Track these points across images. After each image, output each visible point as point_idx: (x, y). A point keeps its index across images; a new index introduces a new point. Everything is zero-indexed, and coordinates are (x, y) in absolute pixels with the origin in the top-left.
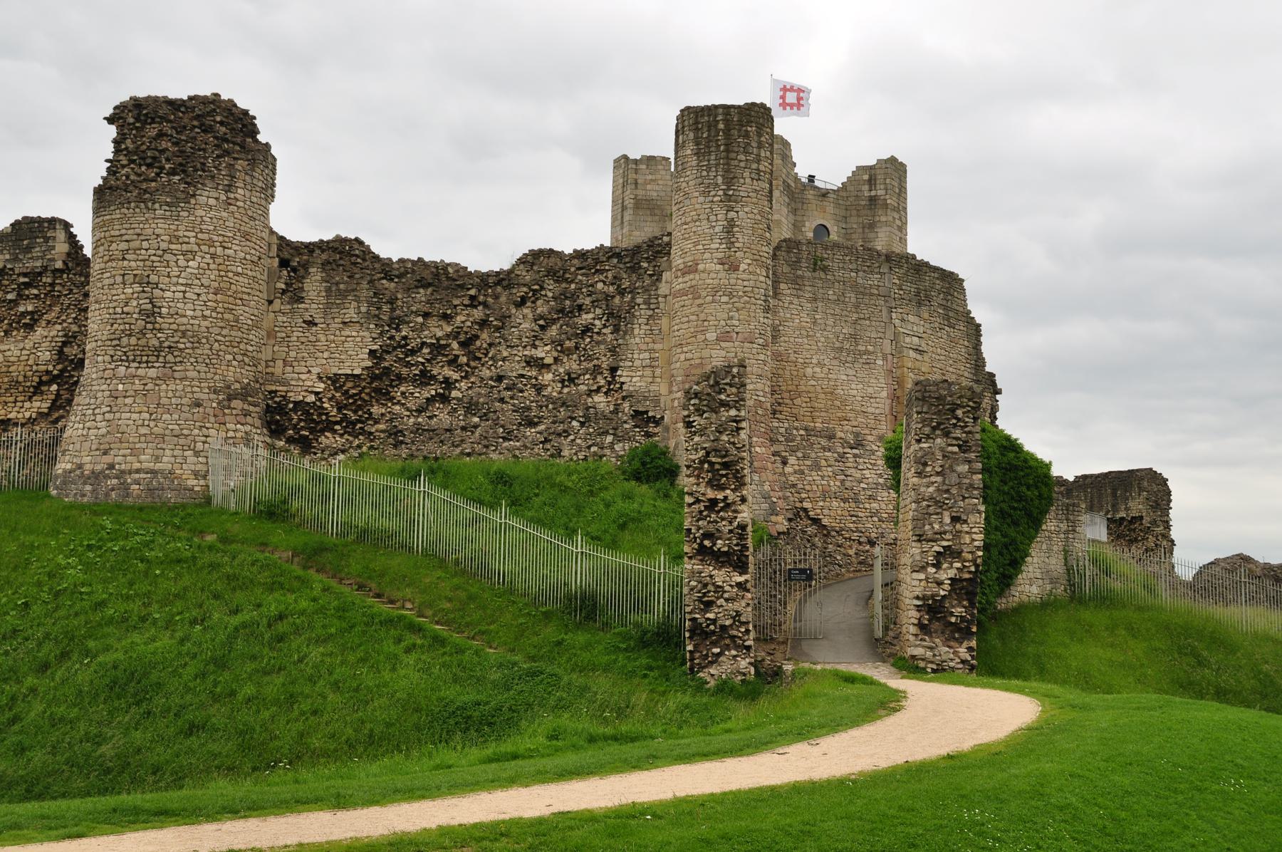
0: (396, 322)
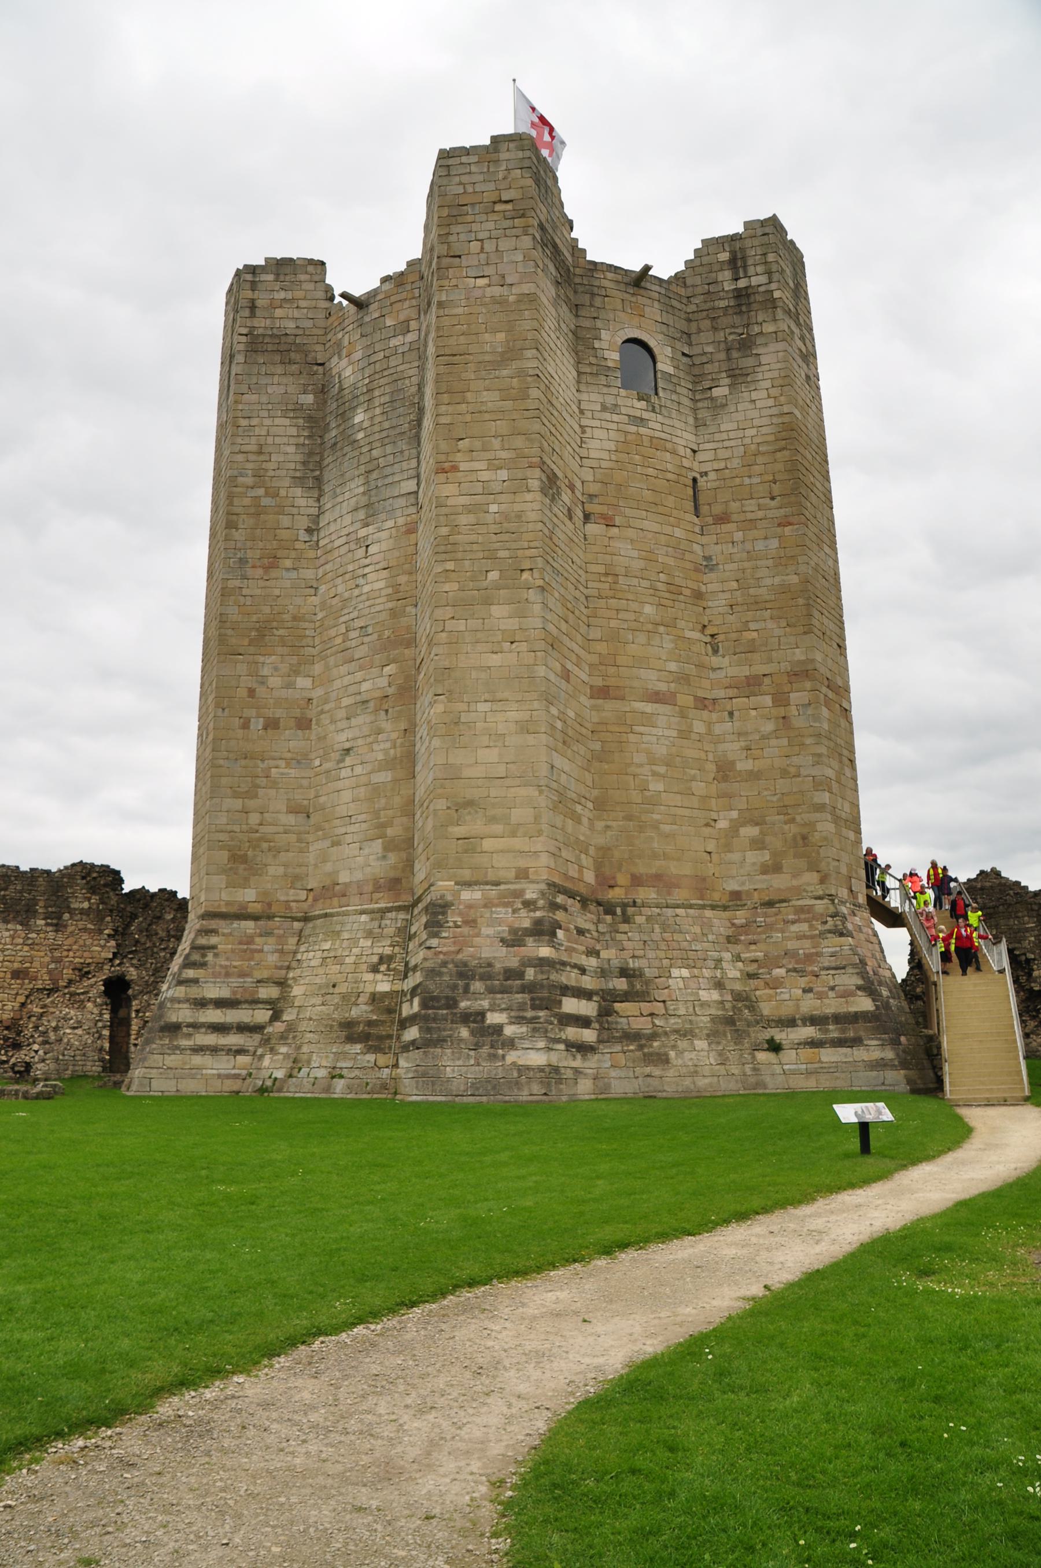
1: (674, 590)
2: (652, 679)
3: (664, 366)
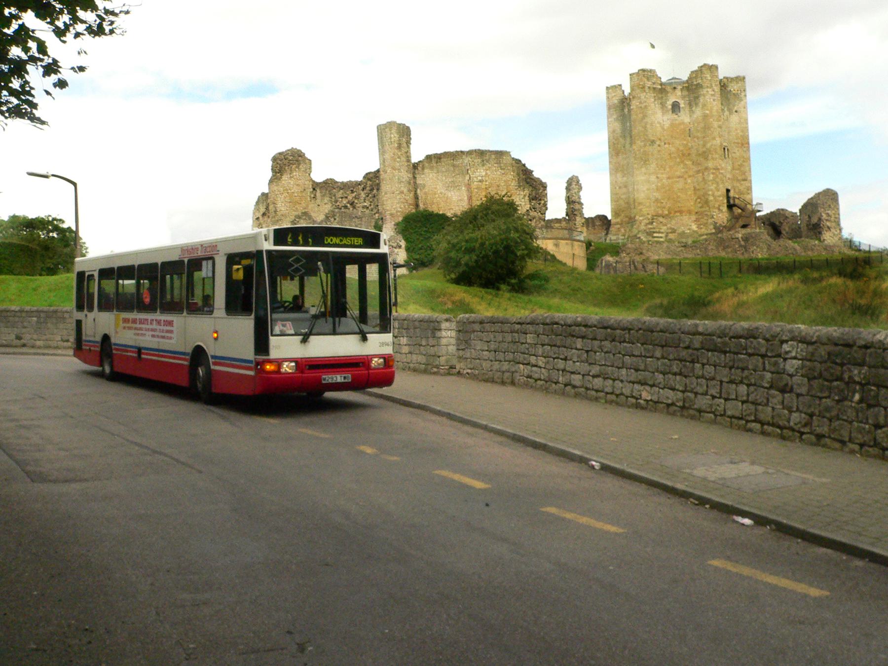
0: (336, 201)
1: (683, 155)
2: (678, 173)
3: (682, 105)
